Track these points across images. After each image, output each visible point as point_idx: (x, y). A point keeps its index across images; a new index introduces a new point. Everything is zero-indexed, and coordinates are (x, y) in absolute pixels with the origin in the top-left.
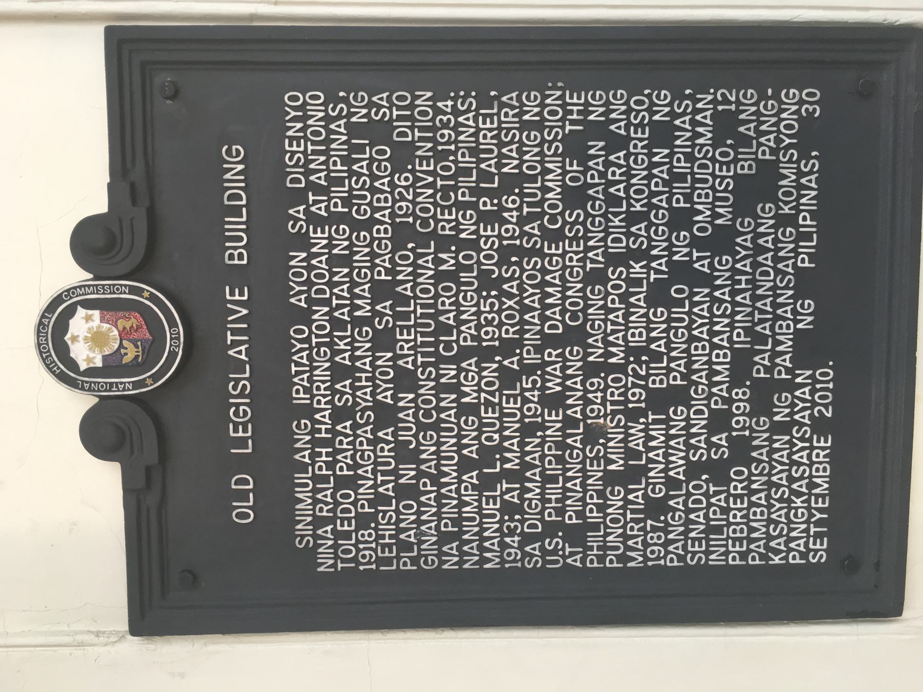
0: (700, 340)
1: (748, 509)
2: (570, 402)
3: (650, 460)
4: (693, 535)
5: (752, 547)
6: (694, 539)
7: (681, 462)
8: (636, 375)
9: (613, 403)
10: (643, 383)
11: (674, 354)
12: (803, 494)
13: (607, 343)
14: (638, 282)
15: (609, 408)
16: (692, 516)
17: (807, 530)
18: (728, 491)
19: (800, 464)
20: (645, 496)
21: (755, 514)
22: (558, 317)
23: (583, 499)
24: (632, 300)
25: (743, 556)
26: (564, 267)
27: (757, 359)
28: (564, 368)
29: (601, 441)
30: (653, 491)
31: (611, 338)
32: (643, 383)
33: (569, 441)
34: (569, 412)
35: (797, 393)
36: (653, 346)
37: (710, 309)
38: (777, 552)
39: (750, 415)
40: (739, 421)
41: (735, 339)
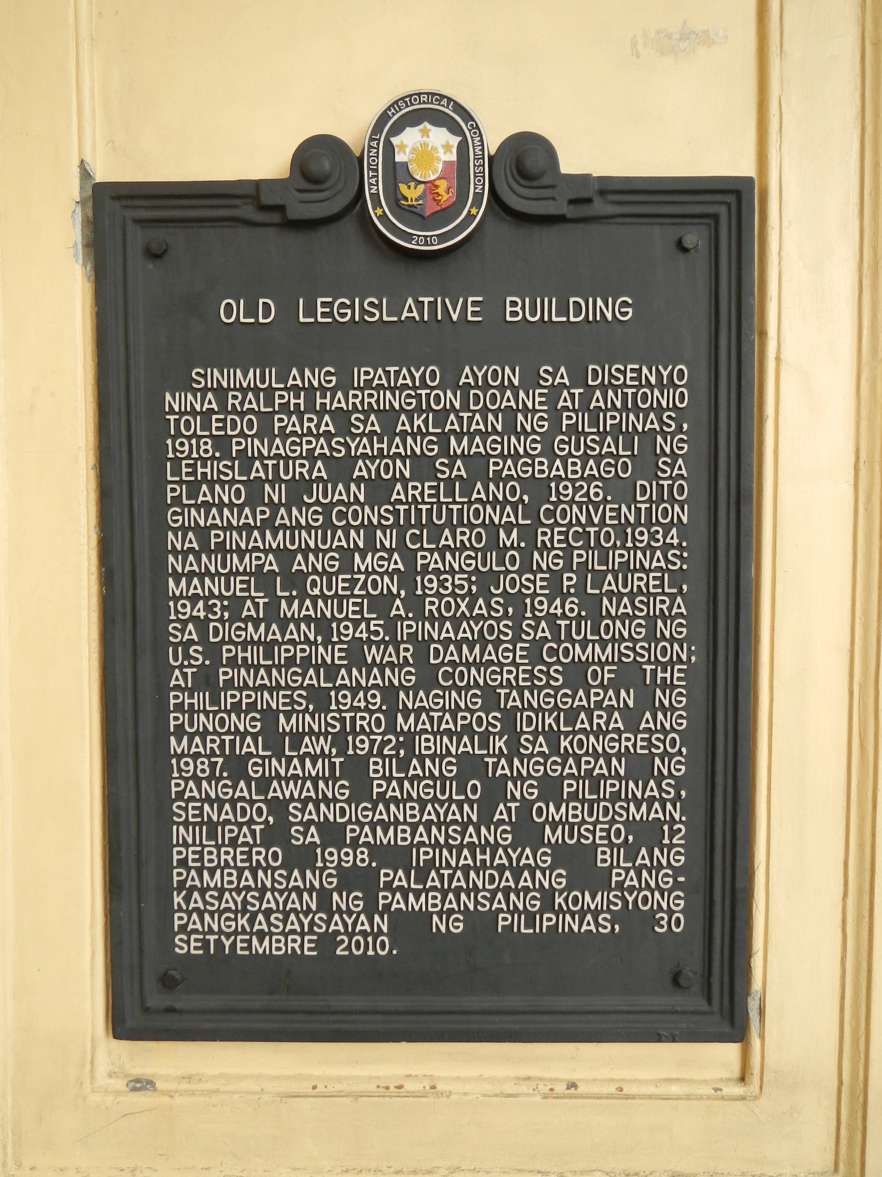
0: (422, 813)
1: (235, 867)
2: (355, 672)
3: (290, 759)
4: (206, 807)
5: (193, 873)
6: (201, 809)
7: (288, 796)
8: (384, 744)
9: (353, 719)
10: (375, 752)
11: (406, 784)
12: (252, 926)
13: (419, 711)
14: (484, 745)
15: (348, 715)
16: (227, 806)
17: (211, 931)
18: (255, 845)
19: (285, 921)
20: (250, 755)
21: (230, 875)
22: (448, 658)
23: (246, 686)
24: (465, 739)
25: (183, 863)
26: (501, 665)
27: (400, 873)
28: (391, 665)
29: (311, 707)
30: (255, 764)
31: (424, 716)
32: (375, 752)
33: (311, 672)
34: (343, 671)
35: (363, 917)
36: (415, 762)
37: (455, 822)
38: (187, 899)
39: (339, 867)
40: (333, 855)
41: (422, 850)
